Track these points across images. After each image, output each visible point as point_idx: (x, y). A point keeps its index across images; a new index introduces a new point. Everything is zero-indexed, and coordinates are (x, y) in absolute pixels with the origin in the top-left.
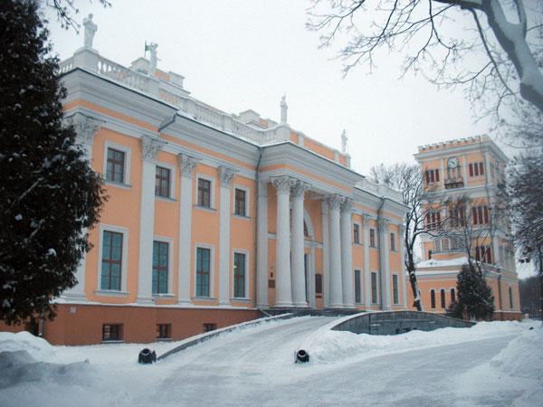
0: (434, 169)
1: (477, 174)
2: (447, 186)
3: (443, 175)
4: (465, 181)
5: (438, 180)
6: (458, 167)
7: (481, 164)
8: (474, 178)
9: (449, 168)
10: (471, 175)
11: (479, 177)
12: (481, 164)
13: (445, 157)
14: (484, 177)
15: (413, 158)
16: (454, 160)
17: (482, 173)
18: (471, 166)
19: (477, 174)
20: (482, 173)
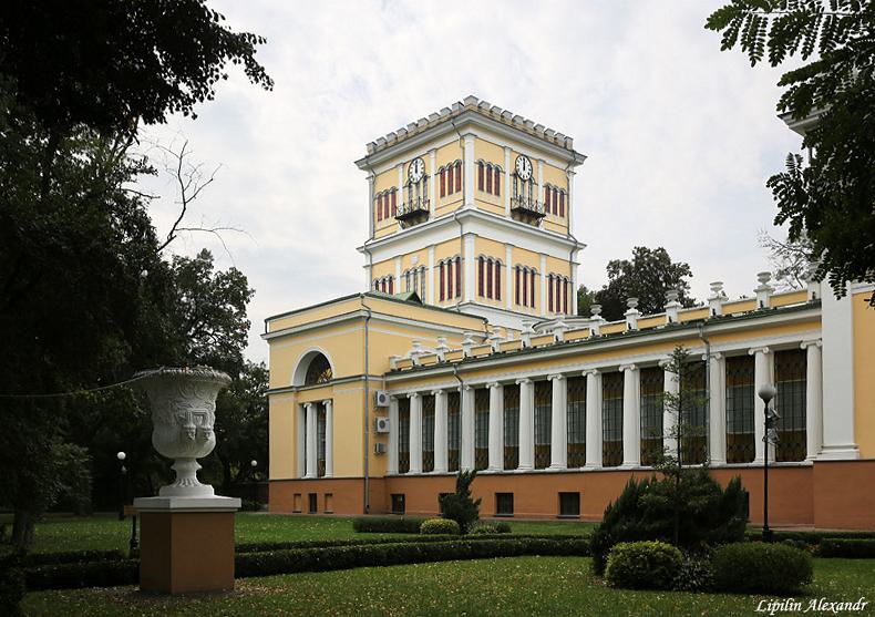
12: (459, 164)
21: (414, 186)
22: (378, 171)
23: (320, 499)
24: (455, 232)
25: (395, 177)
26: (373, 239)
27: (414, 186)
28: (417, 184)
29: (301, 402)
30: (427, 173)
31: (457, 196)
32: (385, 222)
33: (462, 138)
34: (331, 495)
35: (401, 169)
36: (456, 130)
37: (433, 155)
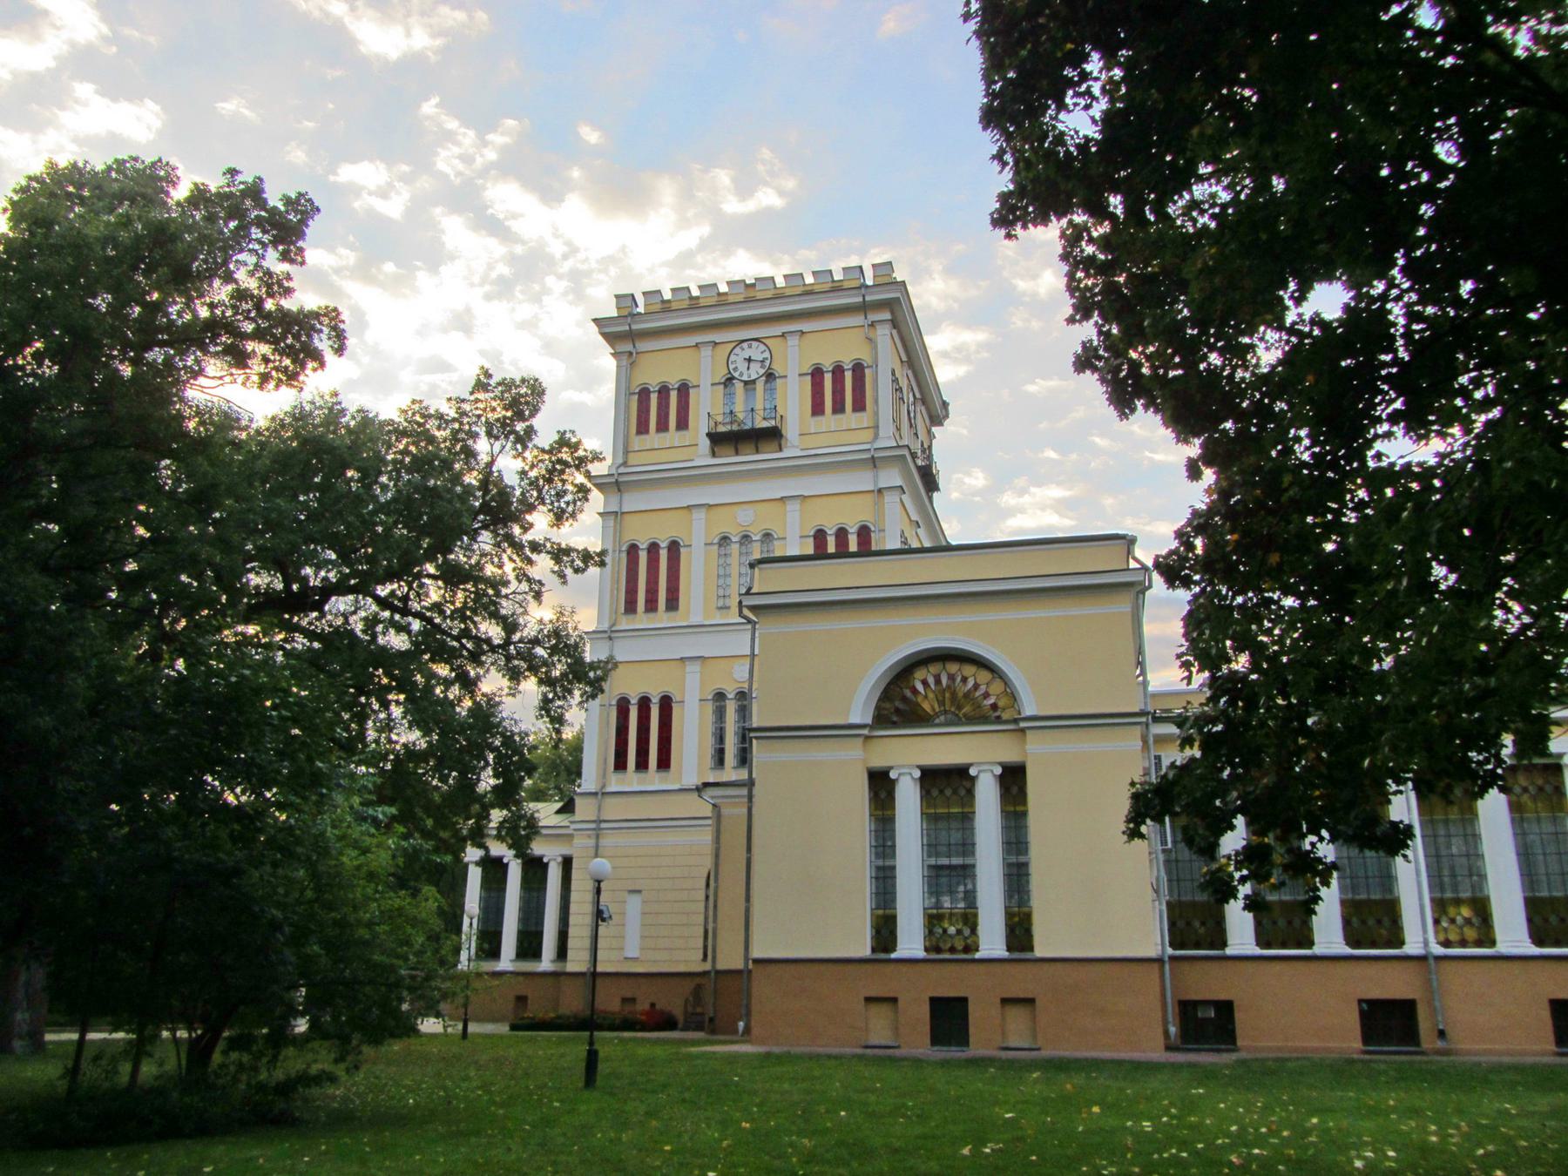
0: (674, 381)
1: (839, 408)
2: (718, 440)
3: (707, 409)
4: (791, 432)
5: (683, 424)
6: (770, 376)
7: (858, 369)
8: (829, 420)
9: (729, 381)
10: (818, 409)
12: (858, 369)
14: (864, 419)
15: (594, 328)
16: (756, 352)
17: (859, 406)
18: (817, 374)
19: (839, 408)
20: (859, 406)
21: (739, 386)
22: (642, 346)
23: (981, 1016)
24: (863, 480)
25: (692, 363)
26: (625, 464)
27: (739, 386)
28: (746, 383)
29: (878, 762)
30: (778, 369)
31: (850, 418)
32: (653, 439)
33: (872, 325)
34: (1029, 1002)
35: (706, 352)
36: (864, 308)
37: (793, 341)
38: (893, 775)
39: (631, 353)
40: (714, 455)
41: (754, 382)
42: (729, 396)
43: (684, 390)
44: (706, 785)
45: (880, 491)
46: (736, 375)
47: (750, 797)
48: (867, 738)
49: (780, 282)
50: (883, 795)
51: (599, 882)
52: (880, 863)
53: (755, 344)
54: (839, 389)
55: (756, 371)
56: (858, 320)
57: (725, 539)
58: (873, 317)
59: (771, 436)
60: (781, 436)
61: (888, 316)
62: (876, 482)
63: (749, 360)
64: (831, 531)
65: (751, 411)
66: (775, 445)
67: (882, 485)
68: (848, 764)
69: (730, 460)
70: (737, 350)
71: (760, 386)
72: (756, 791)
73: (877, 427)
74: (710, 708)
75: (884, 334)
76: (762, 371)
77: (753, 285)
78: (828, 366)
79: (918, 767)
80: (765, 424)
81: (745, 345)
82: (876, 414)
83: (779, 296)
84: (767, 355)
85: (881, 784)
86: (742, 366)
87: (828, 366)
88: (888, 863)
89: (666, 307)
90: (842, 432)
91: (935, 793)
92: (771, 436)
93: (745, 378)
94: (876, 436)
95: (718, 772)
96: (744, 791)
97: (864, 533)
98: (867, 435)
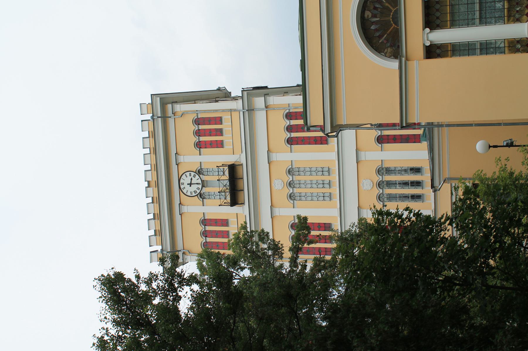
0: (200, 228)
1: (220, 132)
2: (234, 202)
5: (225, 223)
6: (199, 172)
7: (198, 121)
8: (226, 138)
9: (201, 196)
10: (220, 144)
11: (225, 126)
12: (198, 121)
13: (176, 202)
14: (226, 118)
16: (186, 180)
17: (219, 120)
19: (220, 132)
20: (219, 120)
21: (205, 190)
22: (179, 246)
24: (260, 117)
28: (203, 186)
29: (420, 52)
30: (196, 167)
33: (174, 113)
35: (185, 209)
37: (181, 159)
38: (428, 44)
39: (184, 253)
40: (244, 204)
41: (203, 181)
42: (210, 196)
43: (205, 222)
44: (433, 186)
45: (266, 107)
46: (198, 191)
47: (440, 125)
48: (407, 59)
49: (148, 167)
50: (438, 51)
51: (490, 147)
52: (478, 51)
53: (182, 181)
54: (208, 134)
55: (196, 180)
56: (171, 122)
57: (291, 197)
58: (170, 113)
59: (233, 169)
60: (233, 164)
61: (170, 106)
62: (263, 109)
63: (190, 184)
64: (288, 122)
65: (219, 182)
66: (239, 169)
67: (264, 107)
68: (420, 67)
69: (245, 195)
70: (185, 191)
71: (204, 178)
72: (435, 120)
73: (231, 110)
74: (386, 145)
75: (180, 108)
76: (197, 177)
77: (149, 182)
78: (195, 139)
79: (423, 30)
80: (227, 173)
81: (182, 187)
82: (223, 111)
83: (156, 167)
84: (188, 174)
85: (432, 52)
86: (194, 188)
87: (195, 139)
88: (478, 46)
89: (158, 233)
90: (232, 130)
91: (438, 22)
92: (233, 169)
93: (200, 186)
94: (235, 110)
95: (424, 171)
96: (436, 129)
97: (289, 116)
98: (235, 115)
